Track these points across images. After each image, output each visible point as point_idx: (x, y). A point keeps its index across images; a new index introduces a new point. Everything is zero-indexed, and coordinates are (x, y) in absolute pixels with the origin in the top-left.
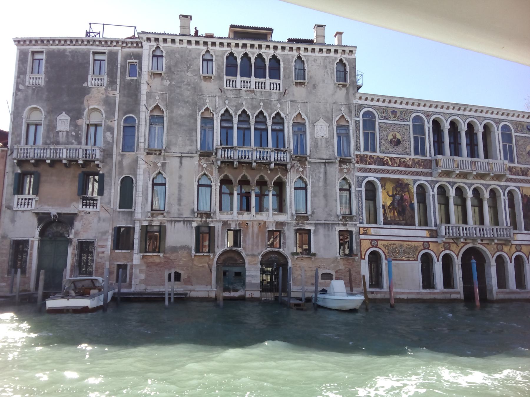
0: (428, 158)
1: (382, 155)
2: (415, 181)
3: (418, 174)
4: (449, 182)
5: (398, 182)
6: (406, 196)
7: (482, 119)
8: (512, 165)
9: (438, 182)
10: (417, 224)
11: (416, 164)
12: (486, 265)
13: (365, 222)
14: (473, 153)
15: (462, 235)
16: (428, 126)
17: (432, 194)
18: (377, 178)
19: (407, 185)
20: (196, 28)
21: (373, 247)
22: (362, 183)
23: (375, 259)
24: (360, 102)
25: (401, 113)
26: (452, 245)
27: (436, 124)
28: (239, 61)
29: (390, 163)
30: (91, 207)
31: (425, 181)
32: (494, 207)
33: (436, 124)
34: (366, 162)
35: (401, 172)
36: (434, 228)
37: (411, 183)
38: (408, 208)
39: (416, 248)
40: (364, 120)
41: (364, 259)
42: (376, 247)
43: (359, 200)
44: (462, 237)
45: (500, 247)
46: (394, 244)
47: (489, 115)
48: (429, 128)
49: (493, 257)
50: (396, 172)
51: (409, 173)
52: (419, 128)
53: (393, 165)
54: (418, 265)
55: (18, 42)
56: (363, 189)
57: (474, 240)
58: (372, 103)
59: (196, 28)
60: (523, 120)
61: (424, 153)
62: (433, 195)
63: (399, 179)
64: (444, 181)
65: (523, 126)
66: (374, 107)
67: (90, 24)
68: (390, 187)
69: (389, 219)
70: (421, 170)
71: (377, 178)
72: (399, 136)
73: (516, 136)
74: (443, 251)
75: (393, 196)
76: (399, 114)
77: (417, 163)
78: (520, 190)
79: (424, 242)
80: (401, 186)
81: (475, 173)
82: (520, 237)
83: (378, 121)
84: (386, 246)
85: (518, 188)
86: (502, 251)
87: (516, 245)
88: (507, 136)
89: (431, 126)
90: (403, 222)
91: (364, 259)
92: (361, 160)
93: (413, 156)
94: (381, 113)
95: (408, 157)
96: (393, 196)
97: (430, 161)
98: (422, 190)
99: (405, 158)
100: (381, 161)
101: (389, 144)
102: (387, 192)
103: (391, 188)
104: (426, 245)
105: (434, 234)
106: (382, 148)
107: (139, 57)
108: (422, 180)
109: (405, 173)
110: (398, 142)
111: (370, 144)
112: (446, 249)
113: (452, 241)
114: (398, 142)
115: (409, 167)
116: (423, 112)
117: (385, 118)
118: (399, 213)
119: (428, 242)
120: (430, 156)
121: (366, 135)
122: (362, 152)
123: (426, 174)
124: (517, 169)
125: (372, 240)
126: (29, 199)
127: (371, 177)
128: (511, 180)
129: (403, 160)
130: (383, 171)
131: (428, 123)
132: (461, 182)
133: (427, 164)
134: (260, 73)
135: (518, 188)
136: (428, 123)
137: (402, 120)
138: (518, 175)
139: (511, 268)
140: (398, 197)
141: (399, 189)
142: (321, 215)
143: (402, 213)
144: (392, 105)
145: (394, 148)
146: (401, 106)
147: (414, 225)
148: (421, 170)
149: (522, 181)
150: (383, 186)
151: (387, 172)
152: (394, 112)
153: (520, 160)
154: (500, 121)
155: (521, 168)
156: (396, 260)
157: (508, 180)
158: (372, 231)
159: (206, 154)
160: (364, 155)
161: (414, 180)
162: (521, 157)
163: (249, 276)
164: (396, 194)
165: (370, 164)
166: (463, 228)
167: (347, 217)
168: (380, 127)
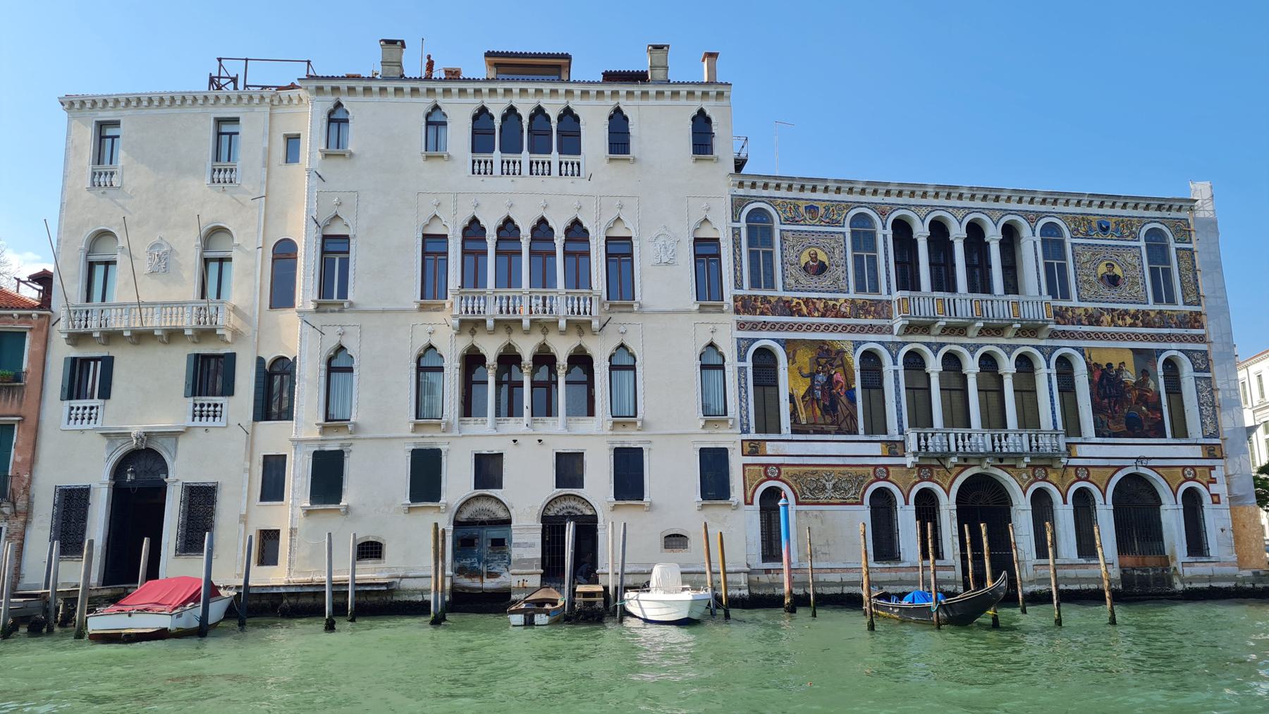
0: (884, 296)
1: (788, 295)
2: (857, 344)
3: (862, 329)
4: (928, 345)
5: (821, 348)
6: (839, 377)
7: (998, 214)
8: (1065, 304)
9: (905, 344)
10: (861, 431)
11: (859, 309)
12: (1013, 509)
13: (753, 430)
14: (980, 282)
15: (953, 449)
16: (884, 233)
17: (892, 370)
18: (777, 341)
19: (841, 352)
20: (429, 57)
21: (769, 478)
22: (746, 352)
24: (741, 192)
25: (827, 209)
26: (935, 470)
27: (902, 229)
28: (497, 122)
29: (805, 310)
30: (211, 418)
31: (879, 342)
32: (1026, 392)
33: (902, 229)
34: (755, 309)
35: (827, 328)
36: (898, 438)
37: (849, 348)
38: (843, 398)
39: (860, 482)
40: (749, 228)
41: (752, 503)
42: (776, 479)
43: (742, 387)
44: (953, 454)
45: (1040, 473)
46: (813, 473)
47: (1013, 205)
48: (885, 236)
49: (1025, 493)
50: (818, 328)
51: (845, 329)
52: (863, 237)
53: (810, 314)
54: (863, 514)
56: (749, 364)
57: (980, 458)
58: (765, 193)
59: (429, 57)
60: (1089, 210)
61: (875, 289)
62: (896, 372)
63: (824, 342)
64: (917, 342)
65: (1090, 222)
66: (771, 200)
67: (220, 60)
68: (805, 358)
69: (804, 422)
70: (870, 321)
71: (777, 341)
72: (822, 257)
73: (1073, 244)
74: (916, 483)
75: (812, 376)
76: (822, 211)
77: (862, 308)
78: (1083, 355)
79: (876, 466)
80: (827, 355)
81: (980, 324)
82: (1083, 451)
83: (777, 227)
84: (797, 477)
85: (1081, 350)
86: (1044, 480)
87: (1077, 467)
88: (1052, 243)
89: (889, 232)
90: (834, 427)
91: (752, 503)
92: (743, 306)
93: (852, 295)
94: (785, 212)
95: (842, 296)
96: (812, 376)
97: (889, 302)
98: (871, 361)
99: (836, 300)
100: (787, 308)
101: (803, 273)
102: (800, 369)
103: (807, 360)
104: (883, 472)
105: (895, 448)
106: (787, 281)
108: (871, 341)
109: (835, 328)
110: (821, 269)
111: (761, 272)
112: (922, 480)
113: (935, 462)
114: (821, 269)
115: (843, 317)
116: (873, 206)
117: (794, 221)
118: (825, 410)
119: (885, 466)
120: (889, 293)
121: (753, 256)
122: (746, 291)
123: (880, 330)
124: (1077, 312)
125: (767, 466)
126: (92, 408)
127: (766, 339)
128: (1065, 335)
129: (831, 303)
130: (790, 327)
131: (884, 227)
132: (953, 344)
134: (540, 143)
135: (1081, 350)
136: (884, 227)
137: (830, 224)
138: (1080, 323)
139: (1064, 515)
140: (821, 378)
141: (823, 361)
143: (830, 408)
144: (808, 194)
145: (814, 281)
146: (826, 196)
147: (856, 433)
148: (870, 321)
149: (1088, 336)
150: (791, 358)
151: (799, 327)
152: (812, 209)
153: (1084, 293)
154: (1040, 215)
155: (1086, 310)
156: (818, 504)
157: (1054, 335)
158: (770, 448)
160: (750, 296)
161: (852, 343)
162: (1087, 286)
163: (518, 545)
164: (818, 372)
165: (762, 313)
166: (956, 435)
168: (783, 239)
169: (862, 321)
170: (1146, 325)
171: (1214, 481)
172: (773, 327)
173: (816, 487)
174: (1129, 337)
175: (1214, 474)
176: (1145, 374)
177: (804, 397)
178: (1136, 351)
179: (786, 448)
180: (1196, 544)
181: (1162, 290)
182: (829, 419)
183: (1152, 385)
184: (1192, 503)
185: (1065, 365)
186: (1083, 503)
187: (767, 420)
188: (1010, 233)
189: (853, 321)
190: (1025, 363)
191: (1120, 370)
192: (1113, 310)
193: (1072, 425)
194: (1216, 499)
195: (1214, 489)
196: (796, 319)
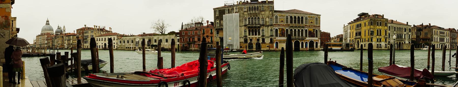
14: (299, 23)
16: (289, 18)
23: (277, 43)
33: (291, 17)
52: (287, 18)
55: (214, 9)
64: (291, 28)
68: (280, 30)
80: (283, 29)
88: (306, 19)
98: (287, 30)
100: (279, 25)
107: (233, 9)
108: (287, 28)
127: (277, 28)
133: (289, 25)
142: (267, 36)
159: (245, 26)
167: (272, 36)
173: (281, 42)
179: (278, 38)
180: (317, 47)
181: (317, 24)
184: (317, 43)
185: (306, 30)
186: (306, 43)
187: (277, 36)
188: (302, 18)
190: (302, 30)
193: (306, 36)
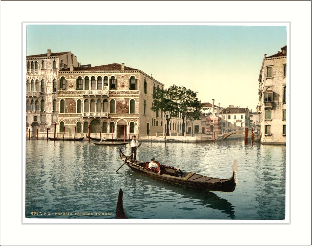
35: (72, 96)
37: (75, 99)
50: (71, 96)
51: (75, 96)
53: (70, 94)
68: (69, 101)
80: (72, 100)
98: (79, 101)
108: (79, 98)
109: (74, 96)
128: (113, 96)
138: (116, 94)
151: (68, 96)
165: (62, 94)
169: (78, 95)
170: (128, 94)
171: (136, 121)
172: (64, 96)
174: (124, 96)
175: (137, 120)
176: (126, 103)
177: (68, 107)
178: (125, 99)
182: (71, 111)
183: (127, 104)
189: (76, 95)
191: (122, 102)
192: (122, 91)
194: (136, 124)
195: (136, 122)
196: (68, 95)
